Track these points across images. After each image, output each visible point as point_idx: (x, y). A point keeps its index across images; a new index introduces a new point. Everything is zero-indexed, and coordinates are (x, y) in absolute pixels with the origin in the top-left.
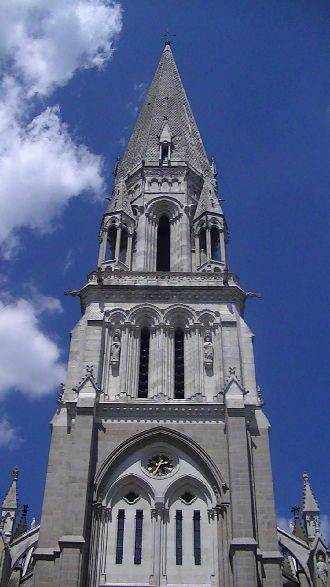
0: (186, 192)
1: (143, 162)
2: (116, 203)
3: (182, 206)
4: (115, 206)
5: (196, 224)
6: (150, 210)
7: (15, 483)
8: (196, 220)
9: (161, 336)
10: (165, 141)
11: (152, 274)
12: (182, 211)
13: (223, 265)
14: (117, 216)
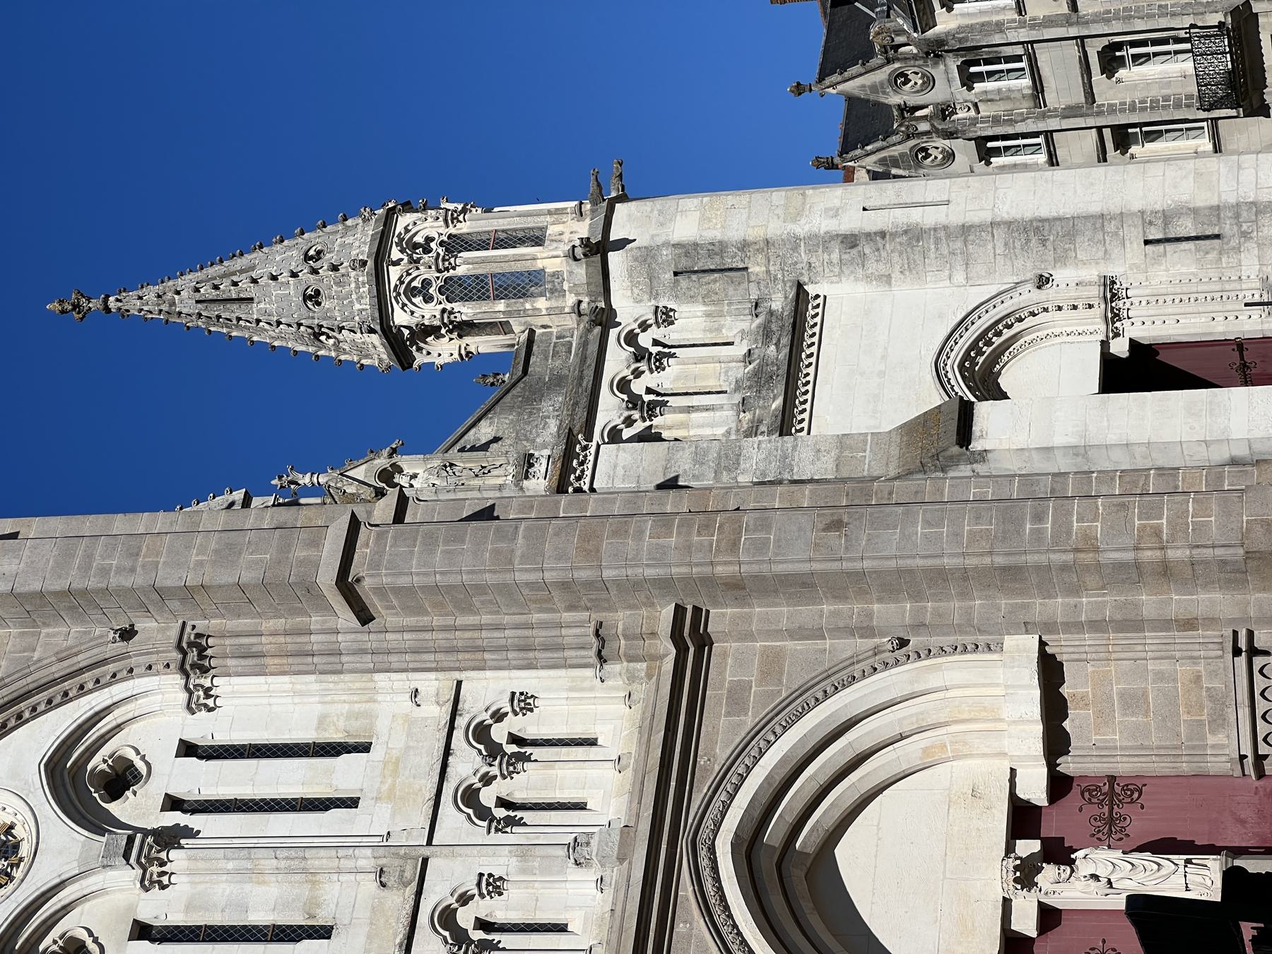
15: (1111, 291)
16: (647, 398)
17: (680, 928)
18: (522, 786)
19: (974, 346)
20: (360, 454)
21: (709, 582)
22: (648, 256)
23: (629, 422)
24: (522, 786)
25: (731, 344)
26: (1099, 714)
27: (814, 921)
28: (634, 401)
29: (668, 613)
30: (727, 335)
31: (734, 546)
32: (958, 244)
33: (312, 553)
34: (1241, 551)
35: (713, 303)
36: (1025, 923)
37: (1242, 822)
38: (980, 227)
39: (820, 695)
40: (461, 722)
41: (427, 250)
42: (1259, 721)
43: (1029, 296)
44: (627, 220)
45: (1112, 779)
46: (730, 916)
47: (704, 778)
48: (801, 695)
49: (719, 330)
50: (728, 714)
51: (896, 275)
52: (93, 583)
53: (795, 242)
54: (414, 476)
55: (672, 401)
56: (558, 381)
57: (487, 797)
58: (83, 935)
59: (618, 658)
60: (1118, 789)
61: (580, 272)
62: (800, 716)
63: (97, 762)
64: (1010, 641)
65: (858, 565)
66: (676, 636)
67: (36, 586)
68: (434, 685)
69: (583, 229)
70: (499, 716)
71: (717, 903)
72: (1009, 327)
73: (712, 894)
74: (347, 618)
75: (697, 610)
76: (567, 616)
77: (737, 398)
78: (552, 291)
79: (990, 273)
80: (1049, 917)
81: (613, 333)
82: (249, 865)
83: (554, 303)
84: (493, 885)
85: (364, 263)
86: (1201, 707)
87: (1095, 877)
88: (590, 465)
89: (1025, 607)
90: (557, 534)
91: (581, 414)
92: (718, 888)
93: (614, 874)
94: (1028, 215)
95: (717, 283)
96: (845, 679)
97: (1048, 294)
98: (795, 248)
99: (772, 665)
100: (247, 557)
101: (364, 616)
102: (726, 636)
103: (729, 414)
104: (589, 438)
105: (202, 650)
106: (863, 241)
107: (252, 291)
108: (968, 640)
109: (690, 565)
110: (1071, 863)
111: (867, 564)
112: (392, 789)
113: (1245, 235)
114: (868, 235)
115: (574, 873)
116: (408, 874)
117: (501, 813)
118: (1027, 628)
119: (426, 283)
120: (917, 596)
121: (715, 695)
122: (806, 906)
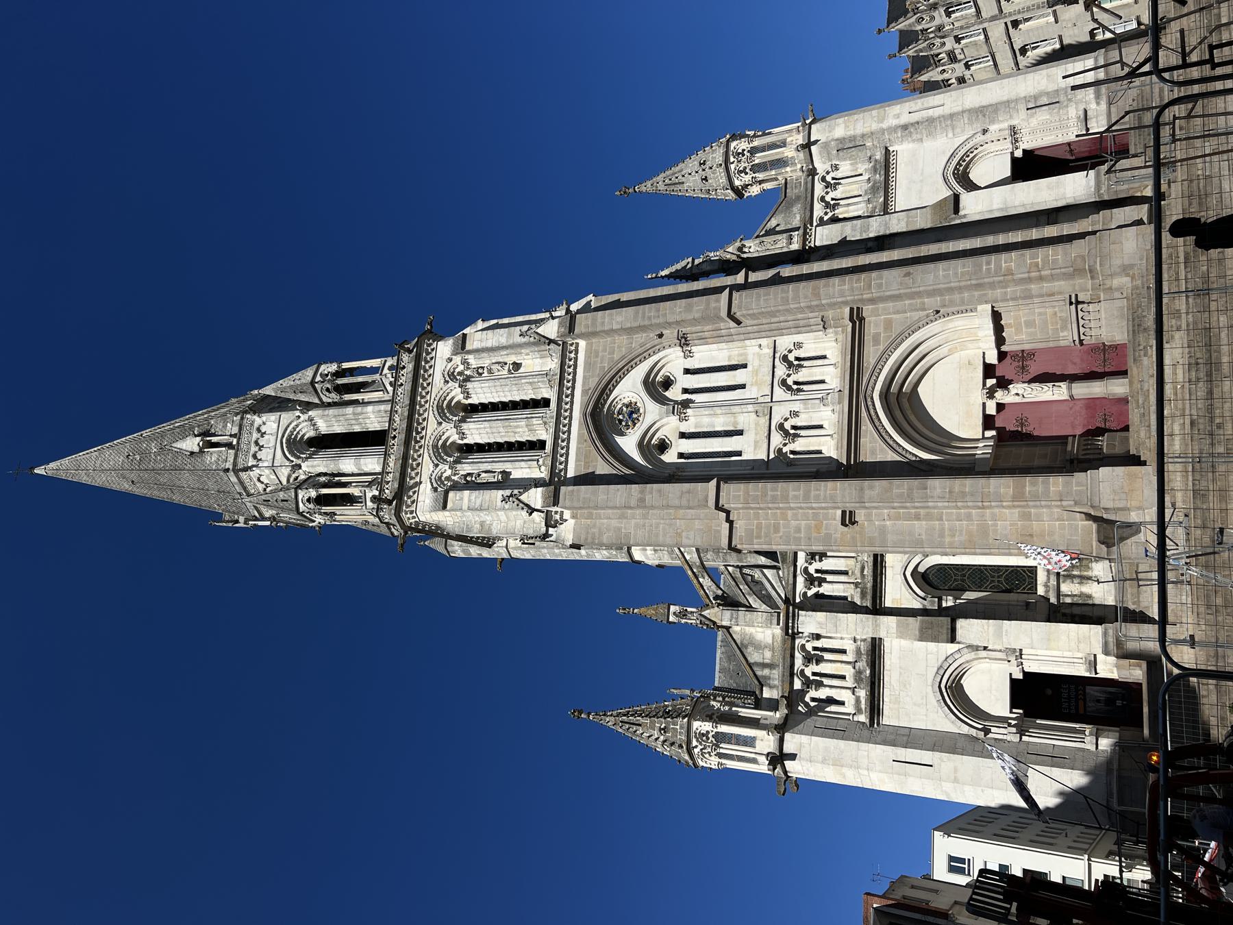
0: (279, 413)
1: (228, 470)
2: (282, 501)
3: (299, 417)
4: (287, 501)
5: (325, 399)
6: (298, 458)
7: (636, 611)
8: (320, 399)
9: (472, 426)
10: (199, 444)
11: (386, 455)
12: (303, 417)
13: (386, 361)
14: (301, 494)
15: (1014, 131)
16: (832, 202)
17: (863, 428)
18: (802, 375)
19: (959, 164)
20: (729, 243)
21: (862, 300)
22: (826, 145)
23: (826, 213)
24: (802, 375)
25: (861, 175)
26: (1016, 329)
27: (912, 418)
28: (827, 205)
29: (847, 310)
30: (859, 172)
31: (870, 286)
32: (949, 122)
33: (718, 304)
34: (1072, 269)
35: (853, 159)
36: (991, 410)
37: (1075, 364)
38: (958, 113)
39: (907, 335)
40: (777, 355)
41: (743, 155)
42: (1081, 328)
43: (980, 138)
44: (817, 132)
45: (1023, 351)
46: (881, 423)
47: (866, 373)
49: (856, 170)
50: (873, 346)
51: (925, 137)
52: (647, 323)
53: (883, 131)
54: (750, 247)
55: (842, 202)
56: (798, 198)
57: (790, 381)
58: (664, 437)
59: (831, 327)
60: (1025, 355)
61: (801, 155)
63: (659, 378)
64: (980, 308)
65: (918, 290)
66: (851, 319)
67: (629, 325)
68: (764, 342)
69: (800, 139)
70: (790, 351)
72: (972, 152)
74: (732, 324)
75: (858, 308)
76: (811, 315)
77: (866, 198)
78: (792, 164)
79: (963, 131)
80: (1000, 407)
81: (816, 177)
82: (712, 412)
83: (793, 169)
84: (795, 414)
85: (721, 165)
86: (1057, 323)
87: (1017, 394)
88: (813, 236)
89: (985, 295)
90: (803, 288)
91: (808, 214)
93: (837, 408)
94: (977, 106)
95: (854, 152)
97: (988, 135)
98: (883, 134)
99: (888, 325)
100: (695, 308)
101: (738, 323)
102: (869, 316)
103: (863, 205)
104: (812, 225)
105: (686, 338)
106: (910, 126)
107: (684, 179)
108: (963, 308)
109: (854, 295)
110: (1008, 389)
111: (921, 289)
112: (756, 382)
113: (1070, 100)
114: (912, 124)
115: (823, 408)
116: (766, 412)
117: (795, 387)
118: (986, 302)
119: (745, 168)
120: (942, 295)
121: (868, 338)
122: (909, 412)
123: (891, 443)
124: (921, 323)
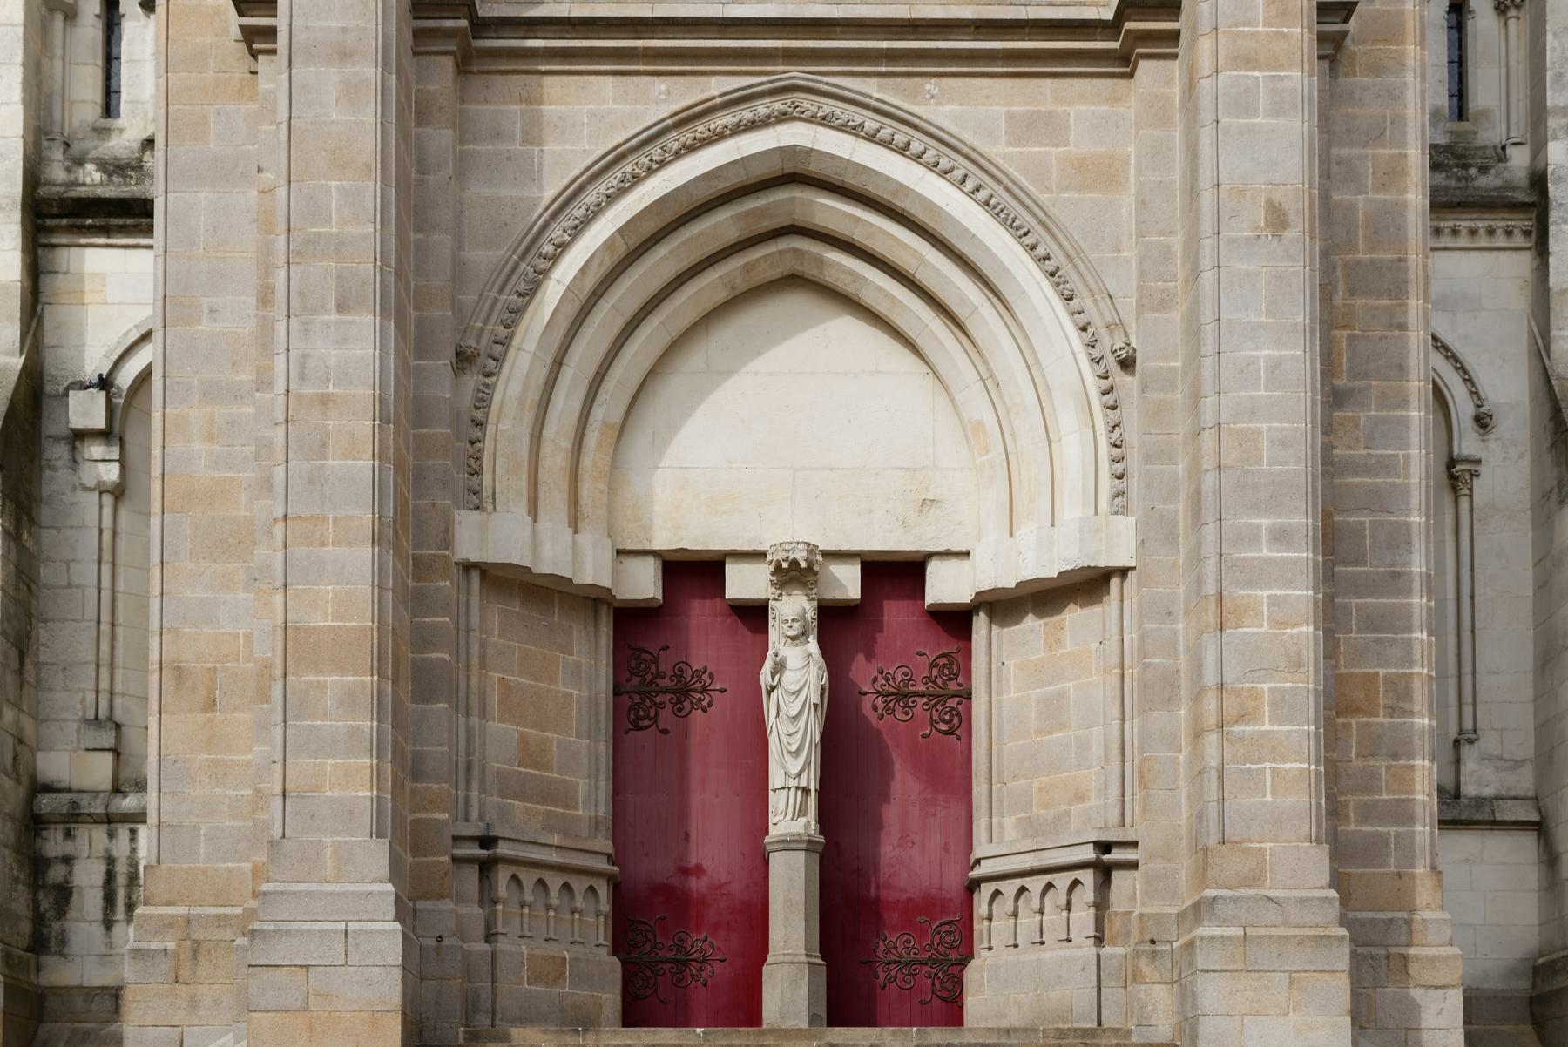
39: (1040, 251)
46: (678, 155)
48: (1040, 221)
62: (1011, 225)
71: (698, 135)
73: (712, 126)
92: (722, 133)
96: (1067, 286)
123: (591, 197)
124: (1088, 303)
